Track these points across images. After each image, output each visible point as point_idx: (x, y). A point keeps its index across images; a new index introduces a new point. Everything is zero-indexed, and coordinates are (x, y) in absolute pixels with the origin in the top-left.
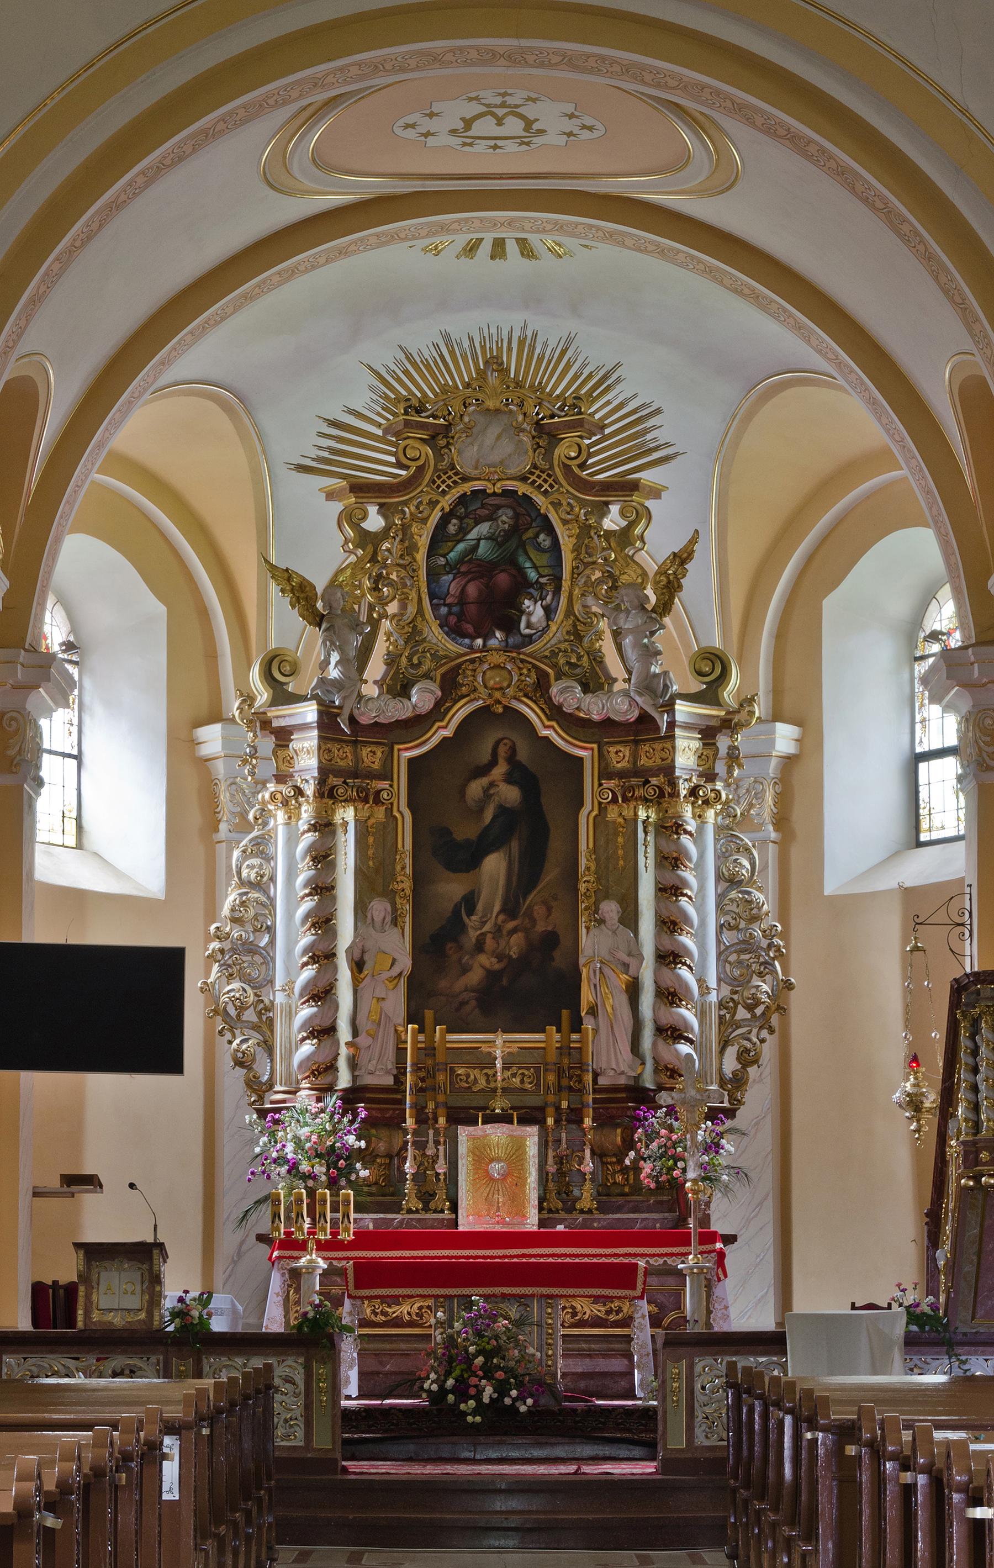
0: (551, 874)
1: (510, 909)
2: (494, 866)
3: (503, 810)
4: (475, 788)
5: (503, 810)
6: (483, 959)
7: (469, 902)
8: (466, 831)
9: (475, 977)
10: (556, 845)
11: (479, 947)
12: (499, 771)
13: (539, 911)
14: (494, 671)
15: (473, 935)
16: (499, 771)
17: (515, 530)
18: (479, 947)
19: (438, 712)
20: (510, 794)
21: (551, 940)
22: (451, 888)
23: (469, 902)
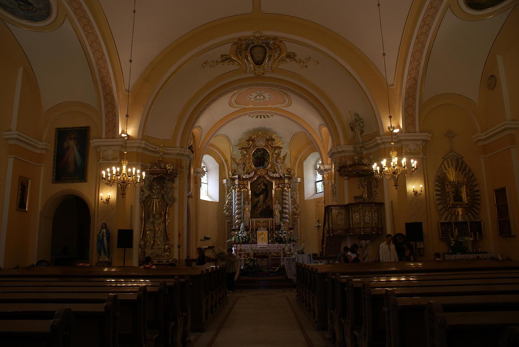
0: (269, 198)
1: (264, 202)
2: (262, 196)
3: (262, 189)
4: (259, 186)
5: (262, 189)
6: (261, 209)
7: (258, 201)
8: (258, 192)
9: (259, 211)
10: (270, 194)
11: (260, 207)
12: (262, 184)
13: (268, 202)
14: (261, 172)
15: (259, 206)
16: (262, 184)
17: (263, 153)
18: (260, 207)
19: (254, 177)
20: (263, 187)
21: (269, 206)
22: (256, 200)
23: (258, 201)
